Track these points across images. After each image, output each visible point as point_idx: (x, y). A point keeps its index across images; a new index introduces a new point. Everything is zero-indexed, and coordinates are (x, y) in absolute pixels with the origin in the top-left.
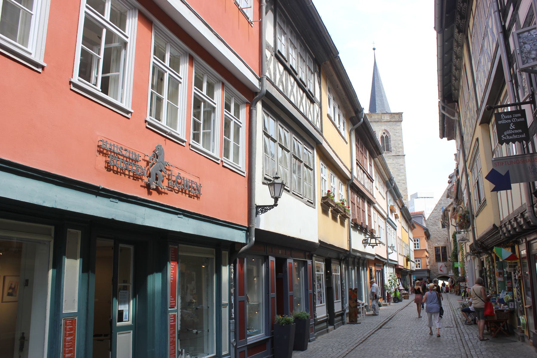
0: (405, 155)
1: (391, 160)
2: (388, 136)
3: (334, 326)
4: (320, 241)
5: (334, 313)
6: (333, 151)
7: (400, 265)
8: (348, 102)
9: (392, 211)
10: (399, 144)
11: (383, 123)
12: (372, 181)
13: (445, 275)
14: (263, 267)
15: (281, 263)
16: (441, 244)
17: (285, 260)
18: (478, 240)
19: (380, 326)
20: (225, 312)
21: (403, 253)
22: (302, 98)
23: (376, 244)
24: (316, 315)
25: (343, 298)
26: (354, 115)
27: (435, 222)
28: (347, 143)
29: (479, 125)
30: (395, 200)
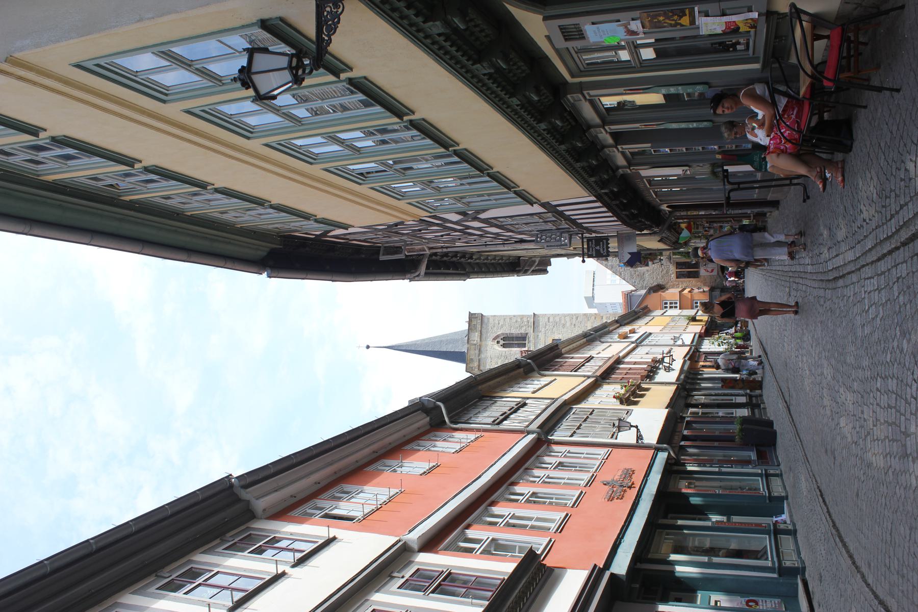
1: (540, 334)
4: (667, 408)
5: (747, 403)
6: (570, 391)
8: (512, 374)
9: (625, 337)
11: (483, 343)
12: (591, 358)
14: (691, 450)
15: (685, 438)
16: (673, 269)
17: (684, 435)
20: (724, 470)
22: (527, 411)
26: (522, 369)
27: (638, 275)
30: (610, 332)
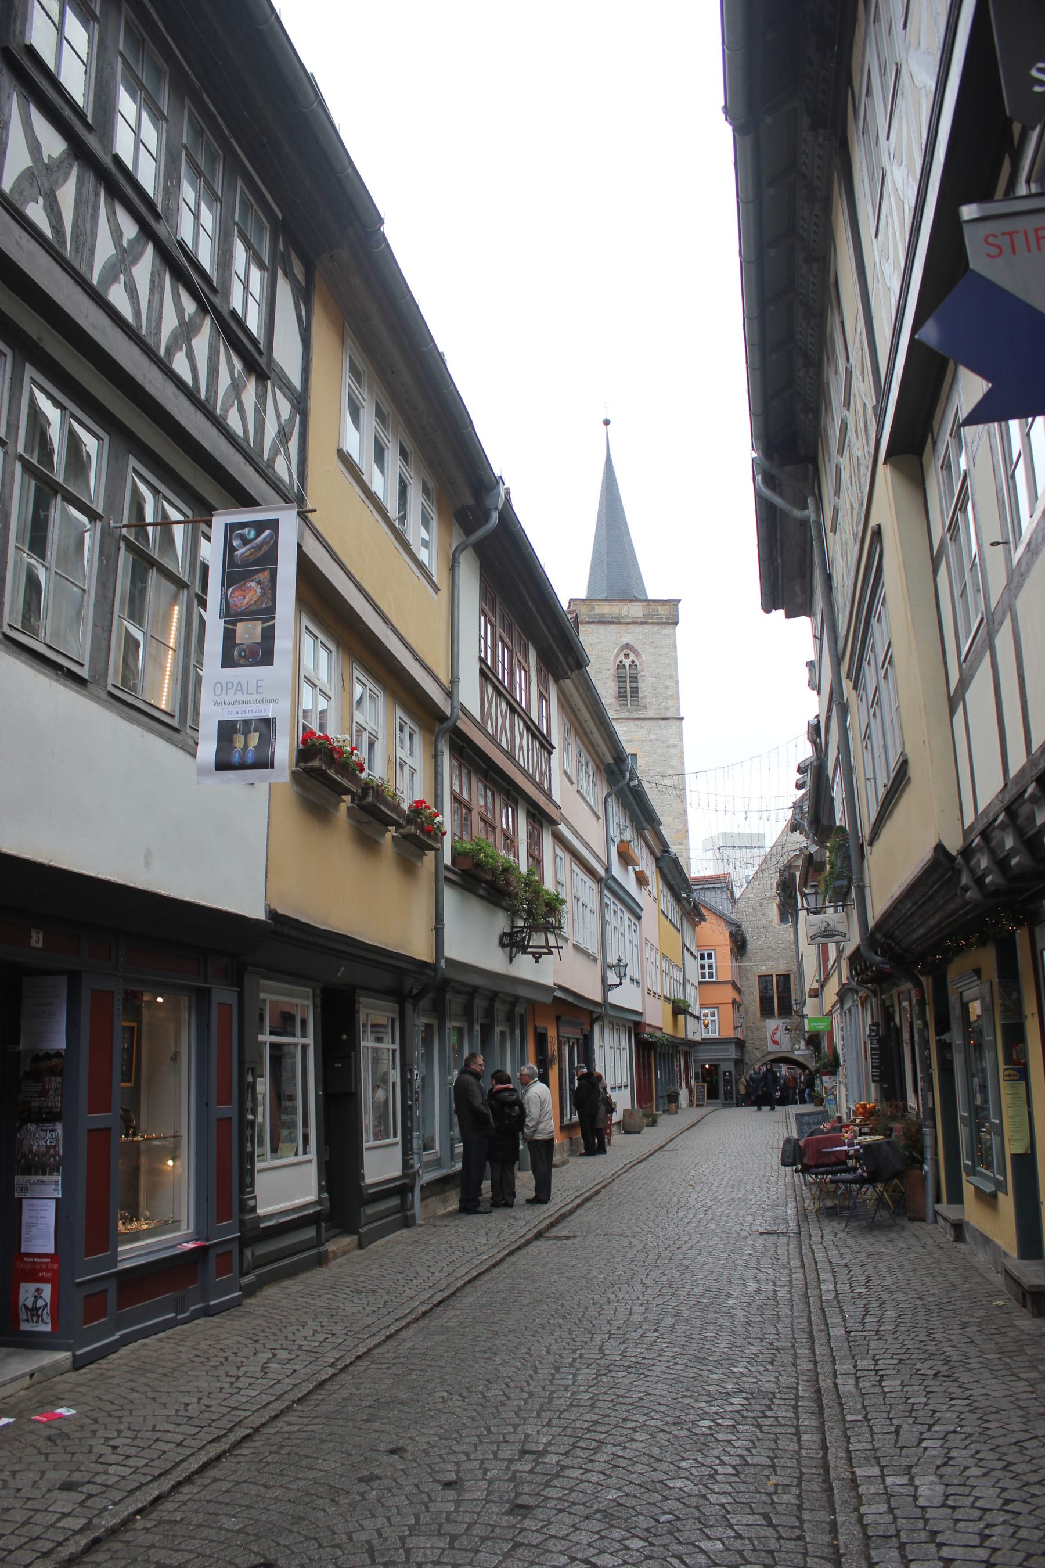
0: (682, 719)
1: (644, 731)
2: (637, 662)
3: (358, 1234)
4: (272, 914)
5: (360, 1189)
7: (650, 1026)
10: (667, 688)
11: (624, 627)
13: (785, 1055)
16: (776, 967)
18: (878, 926)
19: (535, 1231)
23: (546, 950)
24: (251, 1203)
25: (411, 1131)
26: (470, 501)
28: (439, 590)
29: (885, 463)
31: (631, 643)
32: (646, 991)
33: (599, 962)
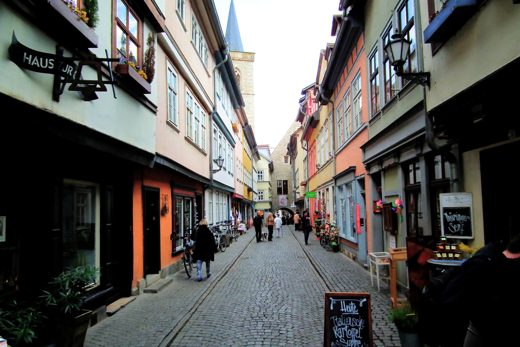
7: (238, 194)
21: (244, 181)
27: (279, 157)
31: (238, 67)
32: (236, 179)
33: (208, 156)
